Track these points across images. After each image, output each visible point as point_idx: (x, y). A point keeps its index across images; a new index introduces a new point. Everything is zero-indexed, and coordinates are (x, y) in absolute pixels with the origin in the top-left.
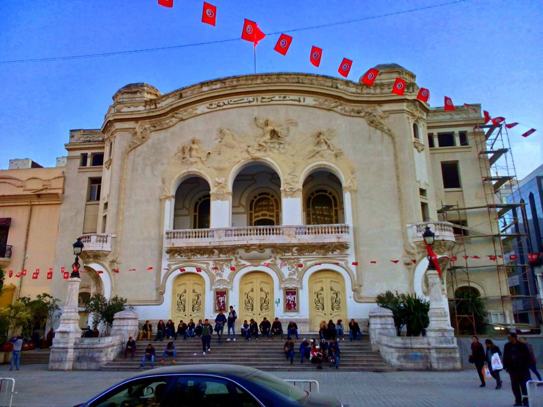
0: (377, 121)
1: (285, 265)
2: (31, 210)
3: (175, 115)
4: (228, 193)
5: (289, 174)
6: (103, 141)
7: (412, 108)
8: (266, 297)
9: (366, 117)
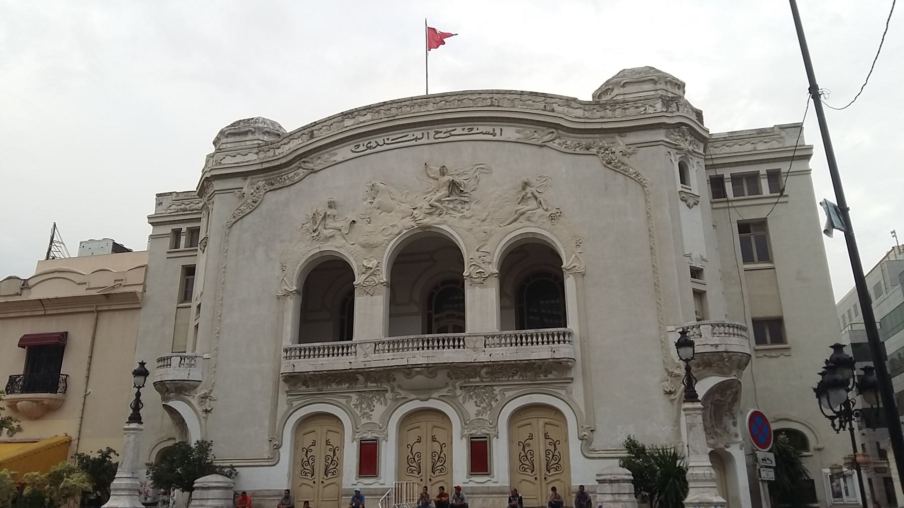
0: (616, 161)
1: (471, 397)
2: (97, 318)
3: (303, 165)
4: (382, 283)
5: (477, 251)
6: (200, 211)
7: (675, 138)
9: (600, 155)
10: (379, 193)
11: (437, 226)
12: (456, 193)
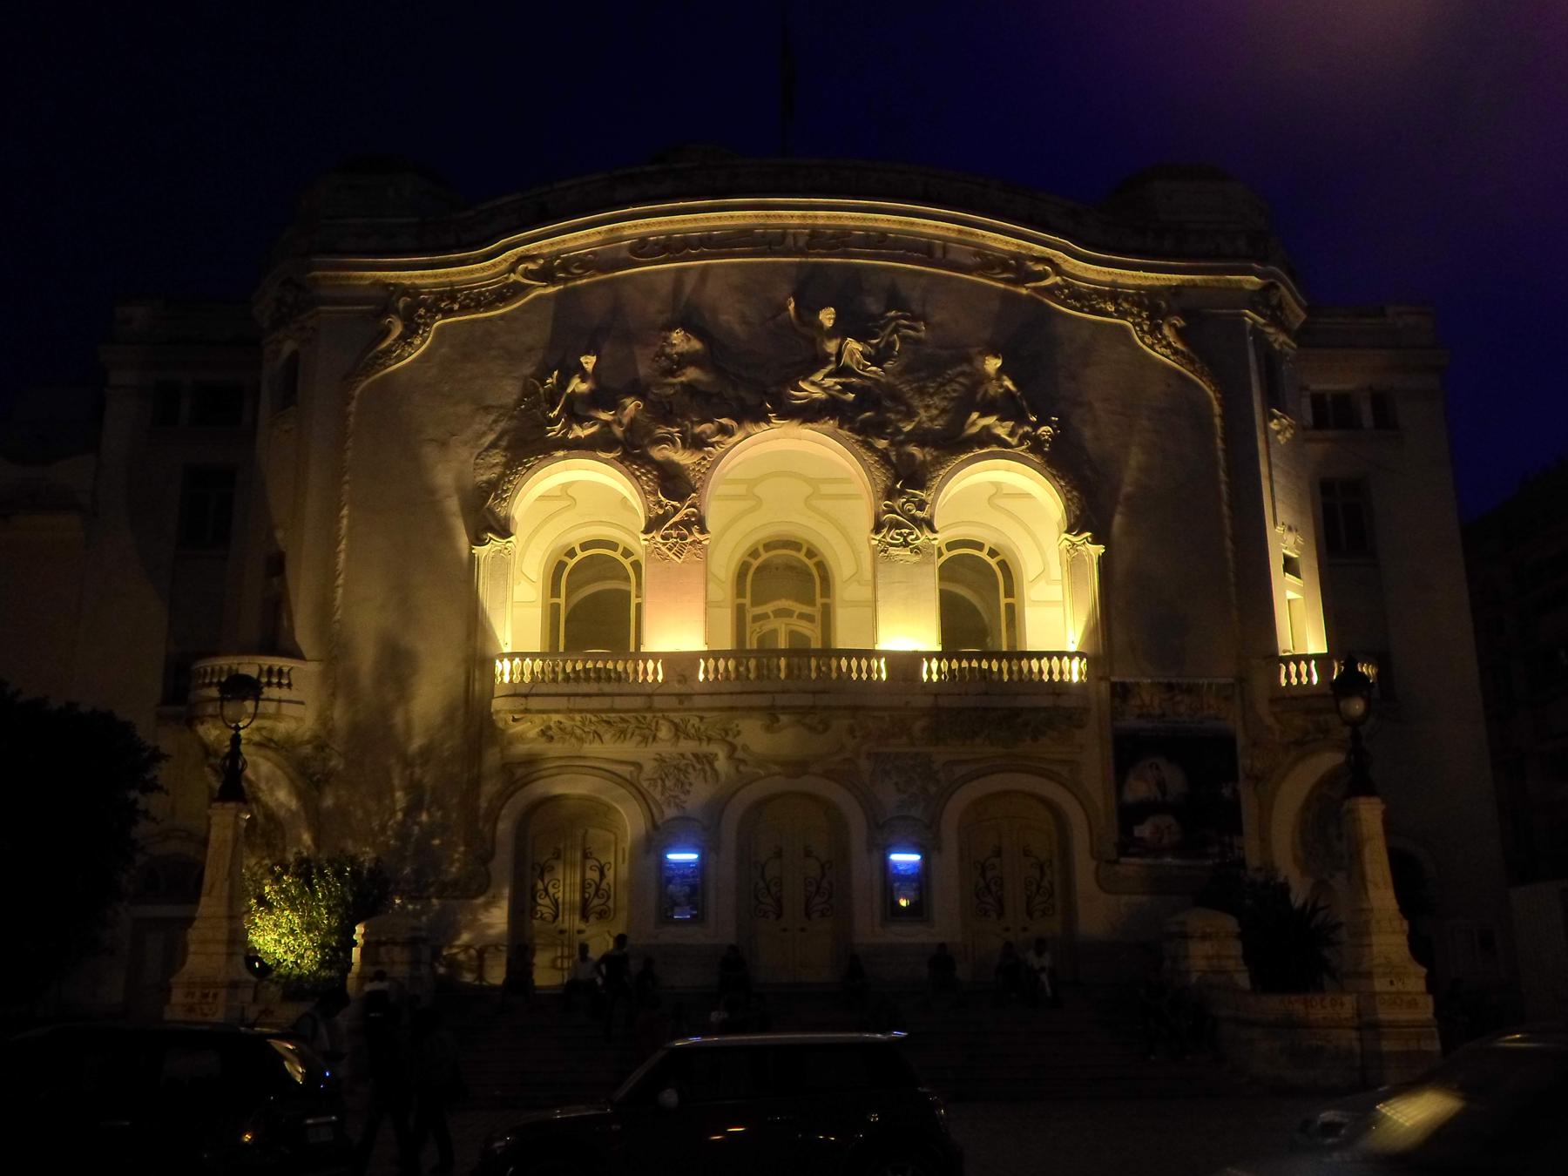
8: (824, 875)
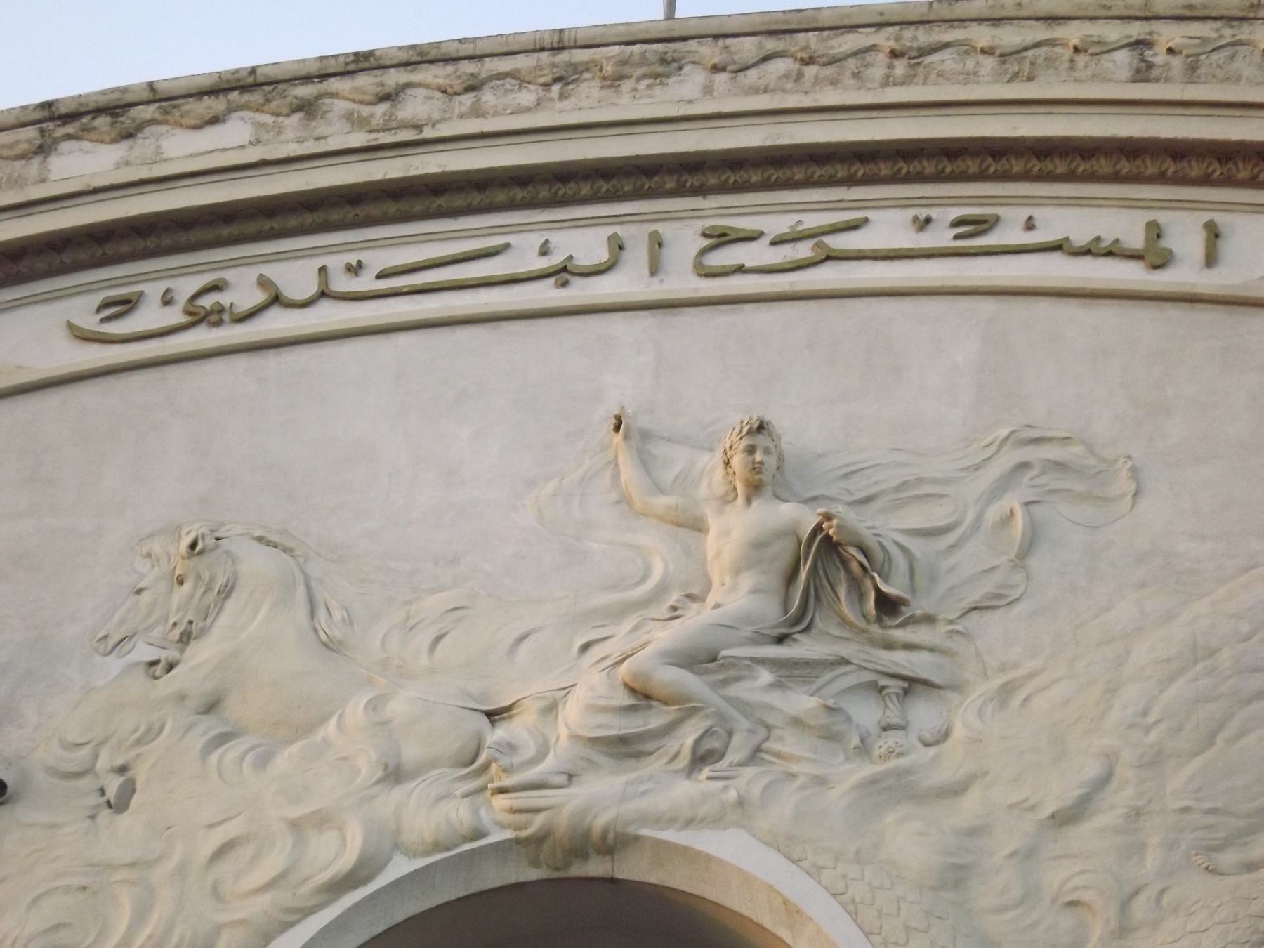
10: (230, 605)
11: (669, 835)
12: (844, 622)
